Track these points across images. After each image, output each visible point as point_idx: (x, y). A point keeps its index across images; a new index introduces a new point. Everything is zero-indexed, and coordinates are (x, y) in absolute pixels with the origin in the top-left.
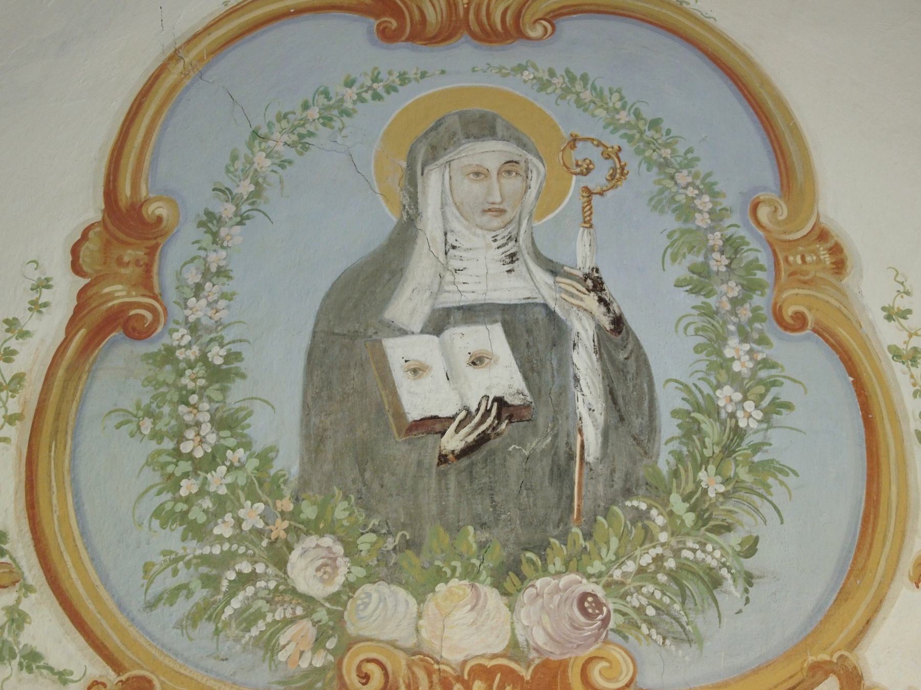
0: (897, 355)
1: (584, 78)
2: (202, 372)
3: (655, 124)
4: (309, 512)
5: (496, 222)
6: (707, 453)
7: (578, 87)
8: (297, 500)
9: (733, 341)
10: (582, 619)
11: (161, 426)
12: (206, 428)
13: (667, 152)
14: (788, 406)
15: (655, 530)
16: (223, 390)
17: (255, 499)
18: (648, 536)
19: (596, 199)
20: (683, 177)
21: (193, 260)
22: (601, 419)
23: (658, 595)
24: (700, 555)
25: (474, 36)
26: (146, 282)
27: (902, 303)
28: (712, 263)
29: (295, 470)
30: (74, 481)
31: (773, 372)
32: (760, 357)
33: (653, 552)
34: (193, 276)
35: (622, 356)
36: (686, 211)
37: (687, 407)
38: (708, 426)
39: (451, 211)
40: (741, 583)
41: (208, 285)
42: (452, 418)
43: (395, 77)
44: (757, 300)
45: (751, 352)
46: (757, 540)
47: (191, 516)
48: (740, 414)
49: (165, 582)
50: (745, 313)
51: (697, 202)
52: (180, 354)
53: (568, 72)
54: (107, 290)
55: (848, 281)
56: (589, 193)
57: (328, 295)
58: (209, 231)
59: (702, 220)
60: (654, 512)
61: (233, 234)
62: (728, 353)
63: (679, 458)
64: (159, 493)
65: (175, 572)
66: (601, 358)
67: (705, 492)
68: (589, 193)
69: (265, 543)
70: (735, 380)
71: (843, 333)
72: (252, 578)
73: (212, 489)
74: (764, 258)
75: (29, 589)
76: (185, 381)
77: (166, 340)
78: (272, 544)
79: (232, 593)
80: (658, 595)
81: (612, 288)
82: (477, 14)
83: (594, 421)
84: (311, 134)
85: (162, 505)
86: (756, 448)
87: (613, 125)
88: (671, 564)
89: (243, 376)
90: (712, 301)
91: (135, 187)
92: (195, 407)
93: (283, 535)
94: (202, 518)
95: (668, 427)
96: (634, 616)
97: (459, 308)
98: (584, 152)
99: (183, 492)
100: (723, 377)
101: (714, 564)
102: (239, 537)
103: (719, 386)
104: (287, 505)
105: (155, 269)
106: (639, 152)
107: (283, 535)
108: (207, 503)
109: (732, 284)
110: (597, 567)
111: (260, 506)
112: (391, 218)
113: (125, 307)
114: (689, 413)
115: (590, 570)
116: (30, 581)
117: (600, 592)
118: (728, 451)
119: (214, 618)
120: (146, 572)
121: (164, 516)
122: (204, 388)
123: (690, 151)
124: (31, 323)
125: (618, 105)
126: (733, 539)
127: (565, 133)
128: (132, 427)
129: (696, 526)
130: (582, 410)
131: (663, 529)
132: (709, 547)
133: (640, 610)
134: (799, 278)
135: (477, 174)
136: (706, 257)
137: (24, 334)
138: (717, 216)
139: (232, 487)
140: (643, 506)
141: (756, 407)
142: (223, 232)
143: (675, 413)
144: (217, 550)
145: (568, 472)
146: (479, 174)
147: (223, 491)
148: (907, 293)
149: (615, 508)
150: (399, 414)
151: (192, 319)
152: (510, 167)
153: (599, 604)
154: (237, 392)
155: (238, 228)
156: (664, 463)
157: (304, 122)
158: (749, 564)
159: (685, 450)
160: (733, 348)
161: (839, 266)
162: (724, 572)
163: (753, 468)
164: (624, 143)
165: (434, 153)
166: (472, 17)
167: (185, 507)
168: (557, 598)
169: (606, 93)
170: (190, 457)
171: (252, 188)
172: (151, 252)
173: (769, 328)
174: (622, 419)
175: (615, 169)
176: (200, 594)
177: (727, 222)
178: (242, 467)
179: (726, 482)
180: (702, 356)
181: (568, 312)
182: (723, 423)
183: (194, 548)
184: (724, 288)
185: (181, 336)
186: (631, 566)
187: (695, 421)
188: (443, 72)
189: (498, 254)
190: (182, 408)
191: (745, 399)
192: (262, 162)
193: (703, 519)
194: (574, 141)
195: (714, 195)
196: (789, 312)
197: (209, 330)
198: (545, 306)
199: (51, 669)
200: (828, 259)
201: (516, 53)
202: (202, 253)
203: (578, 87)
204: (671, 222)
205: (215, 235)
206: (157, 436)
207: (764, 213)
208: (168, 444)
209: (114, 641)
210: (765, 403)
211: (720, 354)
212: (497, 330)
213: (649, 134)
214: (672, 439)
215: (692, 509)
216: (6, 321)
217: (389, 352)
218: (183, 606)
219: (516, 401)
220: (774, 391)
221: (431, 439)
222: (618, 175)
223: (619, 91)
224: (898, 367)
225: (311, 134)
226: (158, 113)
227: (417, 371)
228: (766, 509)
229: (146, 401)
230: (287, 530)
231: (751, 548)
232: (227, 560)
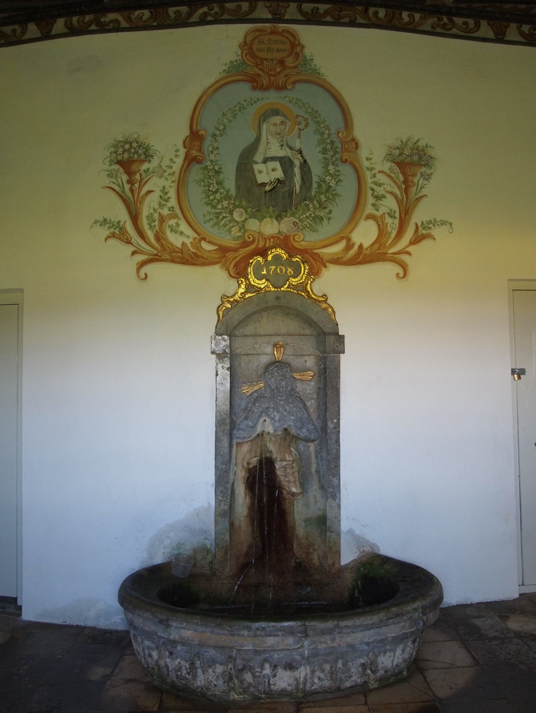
0: (368, 169)
1: (300, 100)
2: (214, 172)
3: (316, 112)
4: (237, 203)
5: (279, 137)
6: (323, 191)
7: (299, 102)
8: (235, 201)
9: (331, 166)
10: (294, 227)
11: (205, 184)
12: (215, 184)
13: (319, 119)
14: (342, 181)
15: (310, 208)
16: (218, 176)
17: (226, 200)
18: (309, 210)
19: (301, 131)
20: (322, 125)
21: (210, 145)
22: (300, 183)
23: (310, 222)
24: (319, 214)
25: (275, 88)
26: (200, 150)
27: (370, 157)
28: (327, 147)
29: (234, 194)
30: (188, 196)
31: (339, 173)
32: (336, 169)
33: (309, 213)
34: (211, 149)
35: (305, 169)
36: (322, 134)
37: (319, 181)
38: (324, 186)
39: (269, 134)
40: (328, 220)
41: (214, 151)
42: (268, 183)
43: (256, 99)
44: (337, 156)
45: (334, 168)
46: (332, 210)
47: (213, 204)
48: (331, 183)
49: (208, 218)
50: (334, 159)
51: (325, 132)
52: (209, 167)
53: (297, 98)
54: (192, 152)
55: (359, 151)
56: (300, 129)
57: (241, 154)
58: (214, 138)
59: (326, 136)
60: (310, 204)
61: (219, 139)
62: (329, 168)
63: (316, 192)
64: (206, 199)
65: (210, 216)
66: (301, 170)
67: (322, 200)
68: (300, 129)
69: (228, 210)
70: (330, 175)
71: (356, 164)
72: (226, 217)
73: (217, 198)
74: (339, 146)
75: (180, 219)
76: (210, 174)
77: (205, 164)
78: (230, 210)
79: (222, 220)
80: (310, 222)
81: (304, 153)
82: (276, 82)
83: (298, 184)
84: (236, 114)
85: (206, 201)
86: (334, 190)
87: (307, 112)
88: (313, 215)
89: (222, 173)
90: (327, 156)
91: (197, 128)
92: (212, 180)
93: (232, 208)
94: (215, 204)
95: (315, 185)
96: (305, 226)
97: (269, 158)
98: (300, 119)
99: (211, 199)
100: (328, 174)
101: (322, 215)
102: (223, 208)
103: (327, 176)
104: (233, 202)
105: (202, 147)
106: (312, 119)
107: (232, 208)
108: (216, 201)
109: (331, 152)
110: (297, 216)
111: (227, 202)
112: (255, 135)
113: (196, 156)
114: (319, 182)
115: (296, 217)
116: (180, 217)
117: (298, 221)
118: (327, 191)
119: (218, 225)
120: (204, 216)
121: (207, 204)
122: (214, 175)
123: (324, 119)
124: (175, 160)
125: (308, 107)
126: (327, 210)
127: (295, 114)
128: (199, 184)
129: (319, 207)
130: (296, 181)
131: (312, 208)
132: (321, 212)
133: (306, 225)
134: (347, 150)
135: (275, 125)
136: (326, 146)
137: (174, 162)
138: (329, 135)
139: (221, 198)
140: (308, 203)
141: (335, 181)
142: (217, 138)
143: (316, 182)
144: (218, 211)
145: (293, 195)
146: (275, 125)
147: (219, 198)
148: (372, 154)
149: (302, 203)
150: (256, 182)
151: (211, 159)
152: (282, 123)
153: (297, 224)
154: (221, 177)
155: (220, 138)
156: (313, 193)
157: (235, 111)
158: (330, 216)
159: (318, 191)
160: (331, 167)
161: (357, 147)
162: (324, 217)
163: (333, 195)
164: (309, 117)
165: (265, 120)
166: (274, 83)
167: (211, 202)
168: (289, 222)
169: (305, 104)
170: (212, 191)
171: (223, 127)
172: (201, 143)
173: (338, 162)
174: (304, 183)
175: (306, 124)
176: (215, 220)
177: (332, 137)
178: (223, 193)
179: (326, 198)
180: (324, 169)
181: (294, 159)
182: (327, 185)
183: (213, 211)
184: (329, 153)
185: (209, 163)
186: (304, 216)
187: (320, 184)
188: (267, 98)
189: (279, 145)
190: (210, 180)
191: (332, 179)
192: (226, 121)
193: (320, 206)
194: (297, 116)
195: (329, 130)
196: (344, 158)
197: (215, 162)
198: (289, 157)
199: (185, 235)
200: (354, 146)
201: (285, 93)
202: (213, 143)
203: (299, 102)
204: (318, 137)
205: (215, 139)
206: (204, 186)
207: (340, 134)
208: (207, 188)
209: (198, 230)
210: (336, 180)
211: (327, 169)
212: (278, 163)
213: (315, 114)
214: (315, 188)
215: (318, 204)
216: (170, 159)
217: (254, 168)
218: (212, 223)
219: (282, 179)
220: (339, 177)
221: (263, 188)
222: (307, 125)
223: (308, 103)
224: (368, 172)
225: (236, 114)
226: (201, 108)
227: (260, 172)
228: (334, 204)
229: (202, 178)
230: (233, 207)
231: (330, 212)
232: (220, 213)
